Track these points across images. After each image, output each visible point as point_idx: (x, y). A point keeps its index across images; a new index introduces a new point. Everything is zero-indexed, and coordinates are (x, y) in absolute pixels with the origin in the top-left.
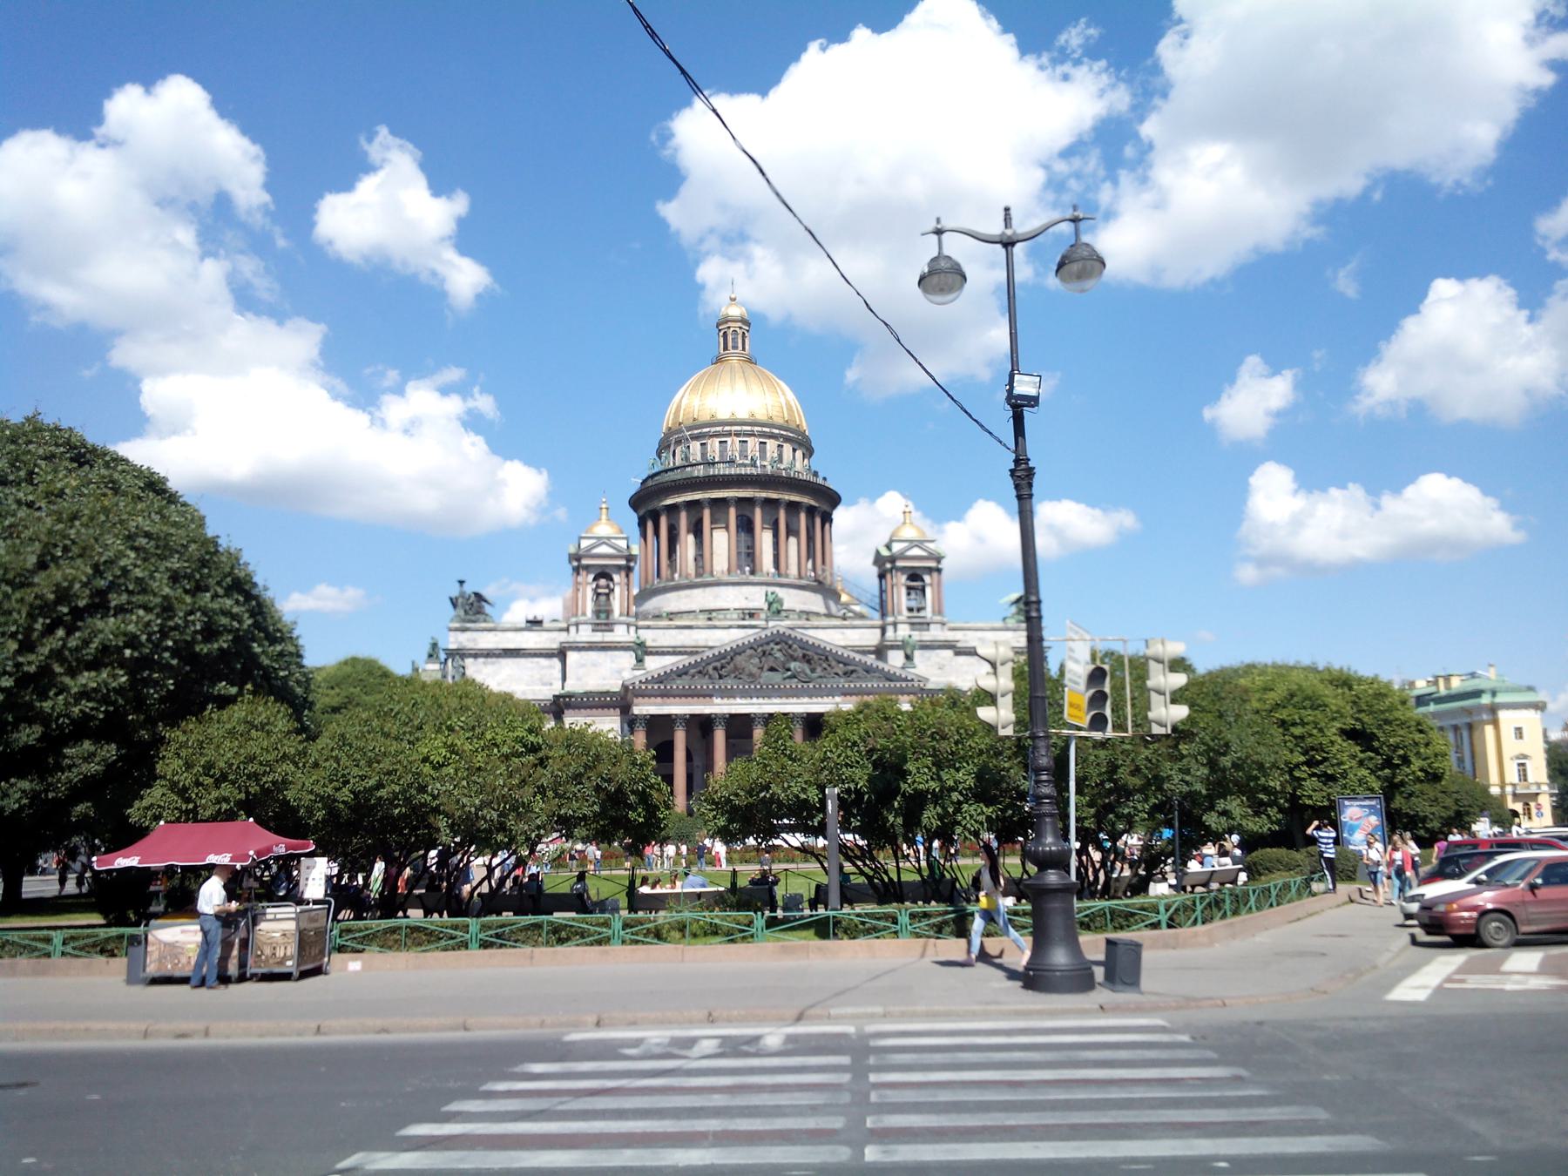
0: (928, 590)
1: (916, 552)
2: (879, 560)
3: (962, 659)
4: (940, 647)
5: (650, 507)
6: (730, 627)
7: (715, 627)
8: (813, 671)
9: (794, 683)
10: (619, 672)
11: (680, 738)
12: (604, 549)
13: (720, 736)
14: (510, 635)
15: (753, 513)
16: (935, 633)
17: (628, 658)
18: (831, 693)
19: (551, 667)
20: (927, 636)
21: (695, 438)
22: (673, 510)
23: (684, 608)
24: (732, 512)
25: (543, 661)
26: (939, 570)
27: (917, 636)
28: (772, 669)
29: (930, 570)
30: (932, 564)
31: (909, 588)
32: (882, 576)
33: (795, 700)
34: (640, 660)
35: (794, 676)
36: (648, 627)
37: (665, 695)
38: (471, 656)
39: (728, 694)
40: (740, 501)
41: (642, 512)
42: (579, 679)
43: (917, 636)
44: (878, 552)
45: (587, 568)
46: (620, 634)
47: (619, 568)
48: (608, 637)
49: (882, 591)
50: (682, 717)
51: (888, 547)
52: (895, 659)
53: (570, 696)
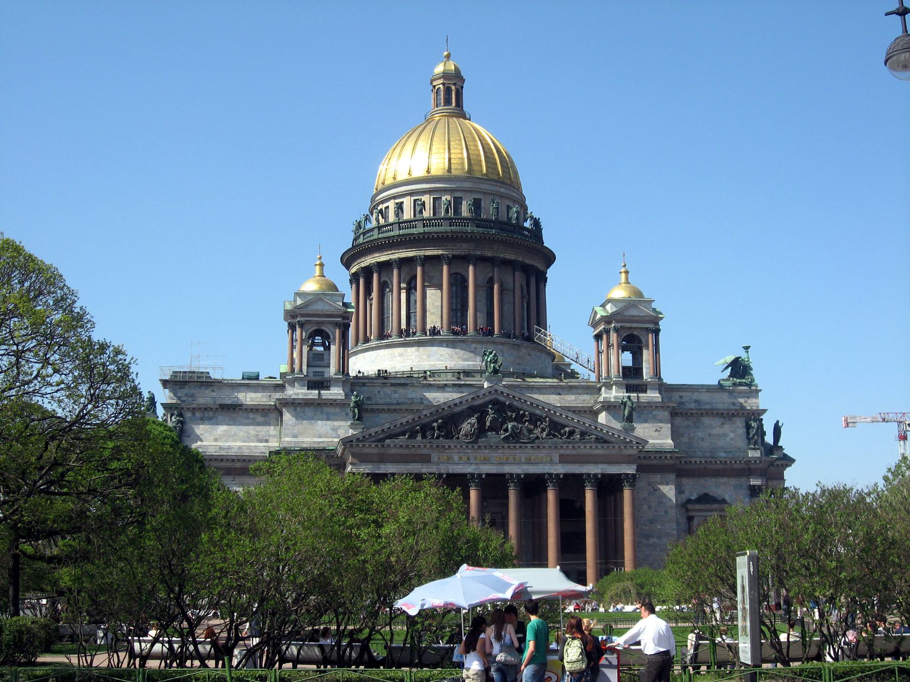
1: (633, 312)
3: (678, 420)
5: (363, 265)
12: (319, 307)
14: (227, 391)
16: (653, 395)
21: (411, 194)
24: (445, 268)
26: (657, 332)
28: (491, 429)
29: (648, 330)
30: (651, 326)
32: (598, 337)
40: (452, 260)
41: (353, 270)
46: (336, 392)
47: (337, 325)
49: (599, 352)
51: (603, 306)
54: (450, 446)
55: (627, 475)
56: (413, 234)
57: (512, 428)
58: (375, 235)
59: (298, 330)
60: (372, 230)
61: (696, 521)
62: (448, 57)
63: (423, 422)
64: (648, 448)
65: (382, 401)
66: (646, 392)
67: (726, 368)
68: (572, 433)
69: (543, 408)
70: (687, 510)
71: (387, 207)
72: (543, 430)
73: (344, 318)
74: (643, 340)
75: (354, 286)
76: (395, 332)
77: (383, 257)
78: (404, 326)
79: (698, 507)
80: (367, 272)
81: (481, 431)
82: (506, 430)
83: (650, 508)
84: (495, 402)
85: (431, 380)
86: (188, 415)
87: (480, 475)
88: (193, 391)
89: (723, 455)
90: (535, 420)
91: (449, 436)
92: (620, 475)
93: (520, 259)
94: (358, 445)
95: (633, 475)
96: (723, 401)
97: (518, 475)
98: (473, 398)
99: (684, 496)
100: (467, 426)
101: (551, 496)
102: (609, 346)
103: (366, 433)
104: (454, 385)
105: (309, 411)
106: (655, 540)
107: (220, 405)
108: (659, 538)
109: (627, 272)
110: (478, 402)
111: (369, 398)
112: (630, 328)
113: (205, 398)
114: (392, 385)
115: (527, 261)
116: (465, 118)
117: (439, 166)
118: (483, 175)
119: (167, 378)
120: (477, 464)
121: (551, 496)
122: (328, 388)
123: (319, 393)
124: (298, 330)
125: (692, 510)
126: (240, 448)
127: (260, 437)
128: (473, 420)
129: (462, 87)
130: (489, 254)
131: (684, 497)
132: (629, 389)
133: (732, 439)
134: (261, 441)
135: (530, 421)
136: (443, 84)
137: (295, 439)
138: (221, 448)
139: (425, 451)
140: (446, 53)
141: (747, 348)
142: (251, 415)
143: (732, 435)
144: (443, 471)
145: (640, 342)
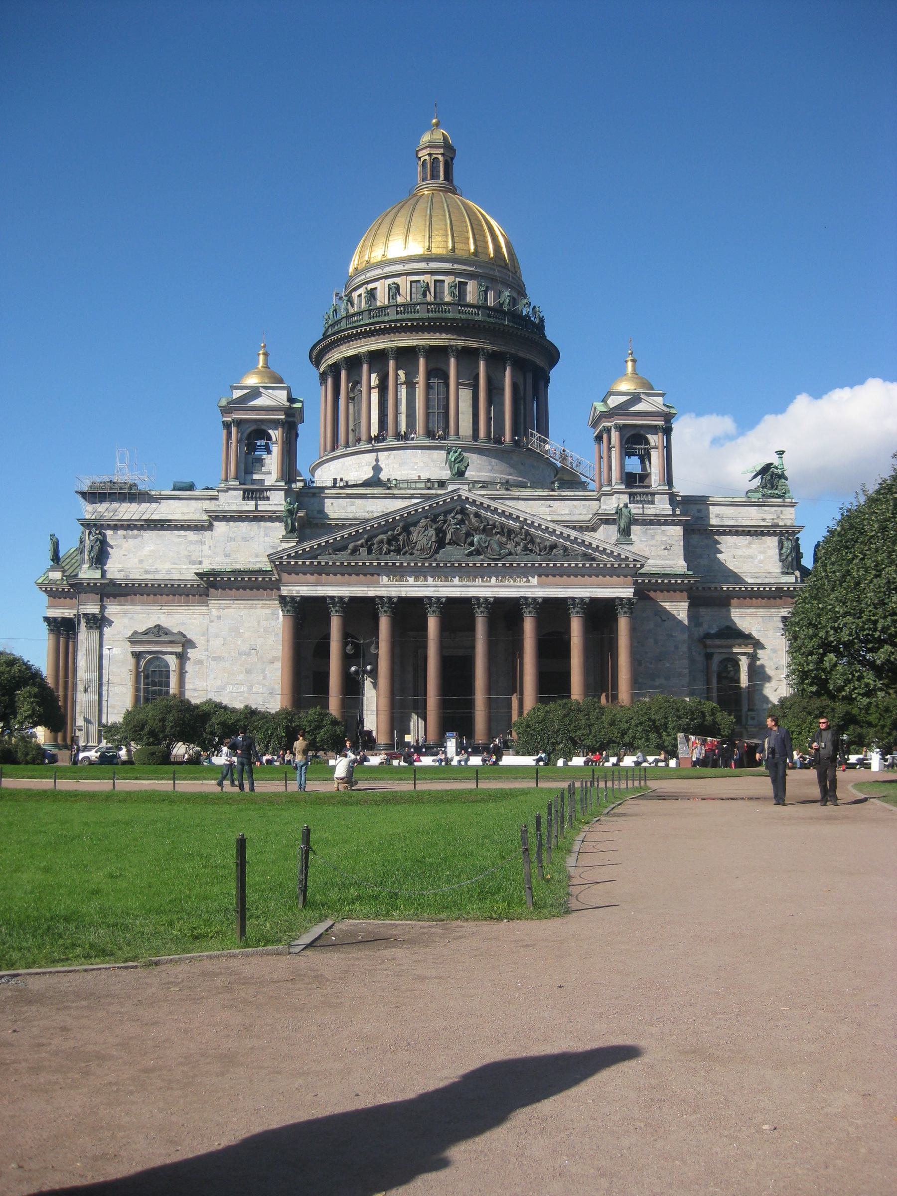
0: (655, 456)
1: (640, 407)
3: (695, 538)
4: (666, 523)
5: (330, 362)
6: (412, 497)
7: (394, 497)
8: (501, 545)
9: (478, 560)
15: (448, 365)
17: (279, 529)
18: (526, 572)
19: (202, 542)
20: (650, 510)
22: (353, 363)
24: (422, 361)
25: (191, 535)
27: (636, 509)
28: (452, 543)
32: (599, 438)
33: (478, 581)
34: (291, 530)
35: (478, 552)
37: (321, 571)
38: (109, 527)
39: (398, 572)
41: (322, 370)
42: (227, 556)
43: (636, 509)
45: (239, 423)
48: (263, 506)
50: (341, 598)
51: (604, 401)
53: (214, 574)
54: (401, 564)
55: (621, 599)
56: (383, 322)
57: (479, 542)
58: (343, 325)
59: (234, 430)
60: (340, 321)
61: (716, 659)
62: (437, 125)
66: (652, 502)
67: (755, 477)
68: (553, 546)
69: (518, 517)
70: (705, 646)
71: (360, 296)
72: (517, 544)
73: (287, 415)
74: (652, 444)
75: (323, 387)
76: (364, 437)
77: (351, 353)
78: (374, 432)
79: (717, 642)
80: (335, 369)
81: (441, 543)
82: (472, 544)
83: (656, 642)
85: (396, 492)
86: (109, 533)
87: (438, 599)
88: (115, 505)
90: (509, 533)
91: (398, 551)
93: (513, 351)
94: (289, 563)
95: (629, 599)
96: (751, 516)
97: (486, 599)
98: (431, 506)
99: (701, 629)
100: (423, 537)
101: (529, 625)
102: (610, 449)
104: (422, 496)
105: (244, 526)
106: (663, 681)
107: (145, 520)
109: (634, 361)
112: (635, 426)
113: (129, 511)
115: (522, 354)
116: (455, 194)
117: (416, 247)
118: (471, 254)
119: (85, 489)
120: (436, 586)
121: (529, 625)
122: (268, 499)
123: (256, 505)
124: (234, 430)
125: (711, 647)
126: (168, 572)
127: (193, 558)
128: (431, 532)
129: (452, 159)
130: (474, 345)
131: (701, 631)
133: (761, 562)
134: (193, 563)
135: (501, 533)
136: (430, 155)
137: (227, 559)
138: (147, 572)
139: (372, 571)
140: (434, 121)
141: (781, 453)
142: (183, 533)
143: (761, 557)
144: (394, 594)
145: (647, 442)
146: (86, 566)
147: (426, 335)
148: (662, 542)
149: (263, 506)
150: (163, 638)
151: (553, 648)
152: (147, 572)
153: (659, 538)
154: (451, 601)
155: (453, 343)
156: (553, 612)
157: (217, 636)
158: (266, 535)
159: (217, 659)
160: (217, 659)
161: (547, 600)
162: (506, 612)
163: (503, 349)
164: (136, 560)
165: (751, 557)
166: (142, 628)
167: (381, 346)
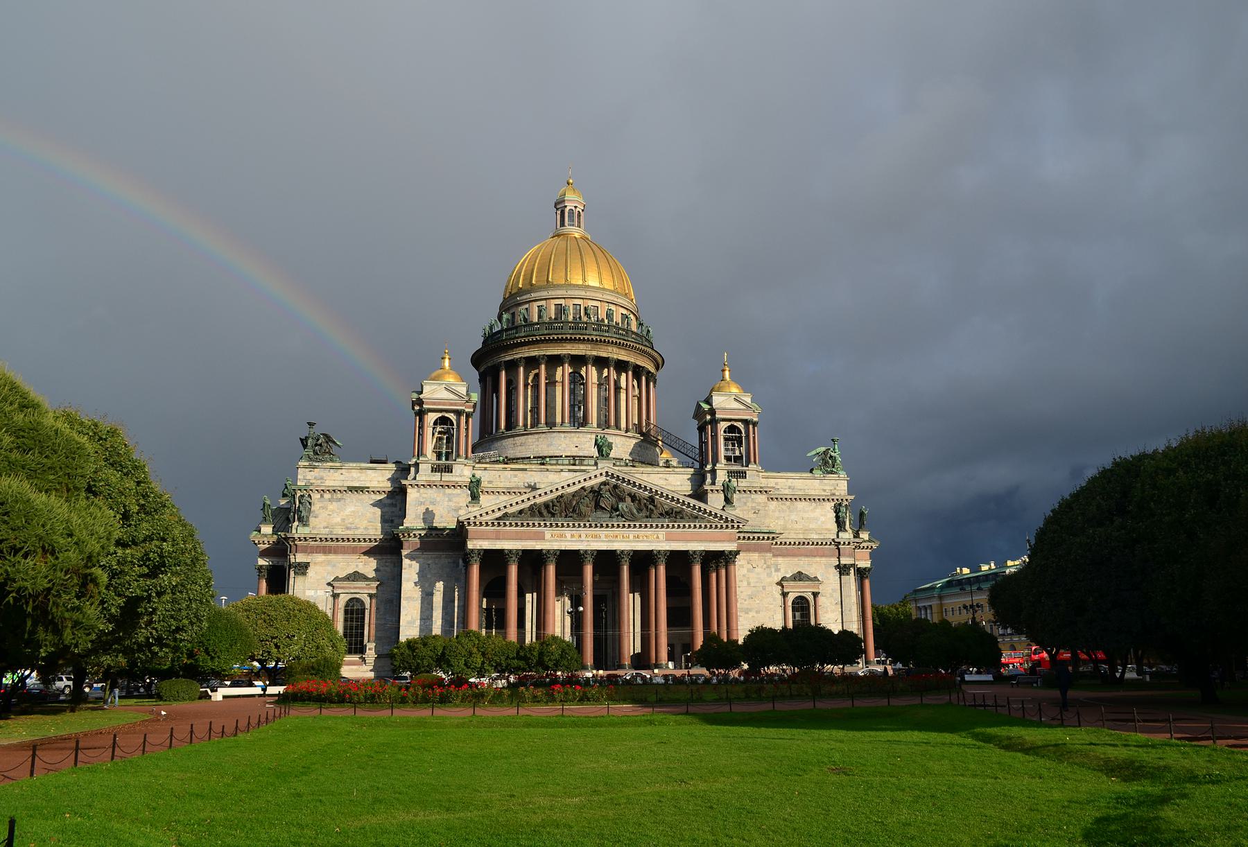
2: (699, 413)
3: (775, 503)
8: (639, 510)
10: (457, 510)
11: (513, 571)
13: (551, 570)
17: (465, 496)
23: (519, 455)
31: (726, 439)
32: (702, 429)
34: (475, 497)
36: (485, 469)
41: (482, 369)
44: (699, 406)
47: (458, 413)
49: (702, 443)
52: (715, 501)
63: (539, 500)
64: (746, 528)
65: (502, 485)
79: (792, 583)
82: (617, 509)
83: (749, 584)
84: (604, 484)
86: (315, 496)
89: (814, 536)
92: (721, 554)
93: (632, 360)
103: (483, 512)
105: (431, 493)
108: (757, 612)
110: (588, 484)
111: (490, 482)
112: (730, 420)
114: (512, 470)
126: (366, 528)
130: (604, 355)
132: (730, 473)
143: (823, 519)
145: (740, 432)
146: (296, 523)
147: (569, 346)
148: (753, 508)
149: (447, 477)
150: (362, 584)
151: (679, 588)
152: (348, 528)
153: (749, 504)
154: (600, 552)
155: (589, 353)
156: (679, 561)
157: (408, 580)
158: (450, 500)
159: (407, 599)
160: (407, 599)
161: (672, 552)
162: (643, 561)
163: (625, 358)
164: (339, 520)
165: (816, 519)
166: (342, 575)
167: (533, 354)
